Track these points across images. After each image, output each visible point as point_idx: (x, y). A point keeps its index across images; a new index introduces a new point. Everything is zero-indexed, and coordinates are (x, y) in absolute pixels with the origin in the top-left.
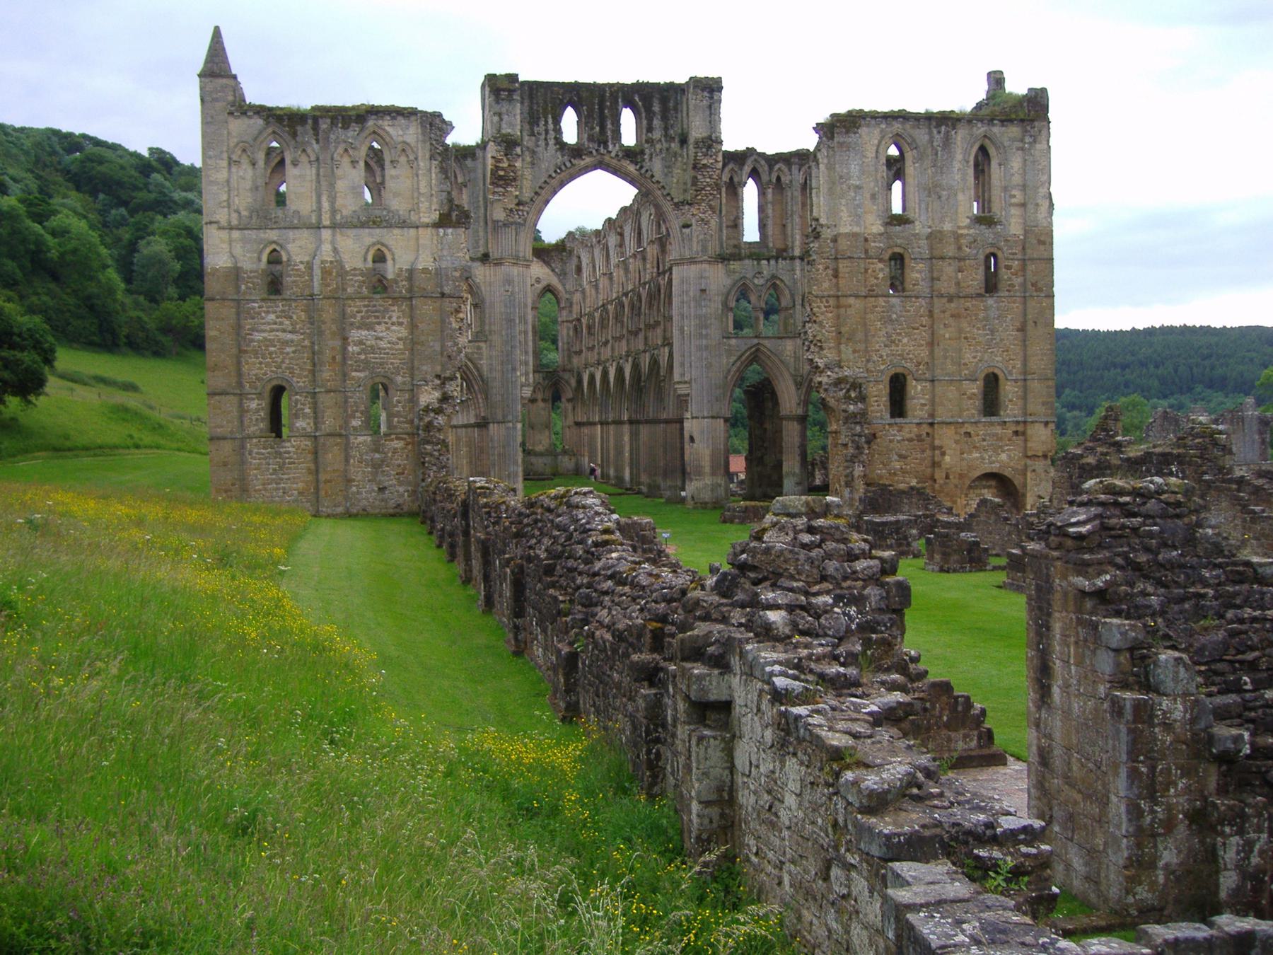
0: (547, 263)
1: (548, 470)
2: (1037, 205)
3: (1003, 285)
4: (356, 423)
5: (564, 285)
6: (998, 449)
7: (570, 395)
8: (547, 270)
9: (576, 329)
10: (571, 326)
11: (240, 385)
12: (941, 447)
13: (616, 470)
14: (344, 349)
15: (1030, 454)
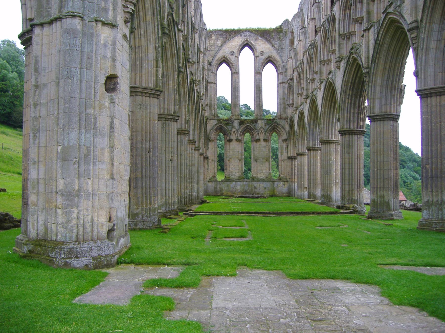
0: (269, 41)
1: (267, 193)
5: (281, 57)
7: (285, 137)
8: (268, 46)
9: (289, 87)
10: (286, 86)
13: (323, 189)
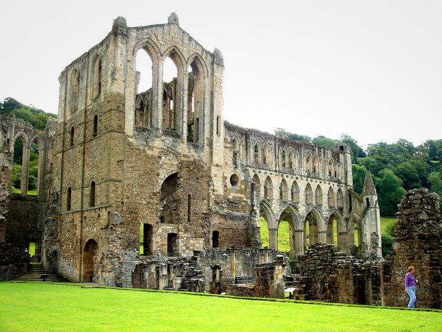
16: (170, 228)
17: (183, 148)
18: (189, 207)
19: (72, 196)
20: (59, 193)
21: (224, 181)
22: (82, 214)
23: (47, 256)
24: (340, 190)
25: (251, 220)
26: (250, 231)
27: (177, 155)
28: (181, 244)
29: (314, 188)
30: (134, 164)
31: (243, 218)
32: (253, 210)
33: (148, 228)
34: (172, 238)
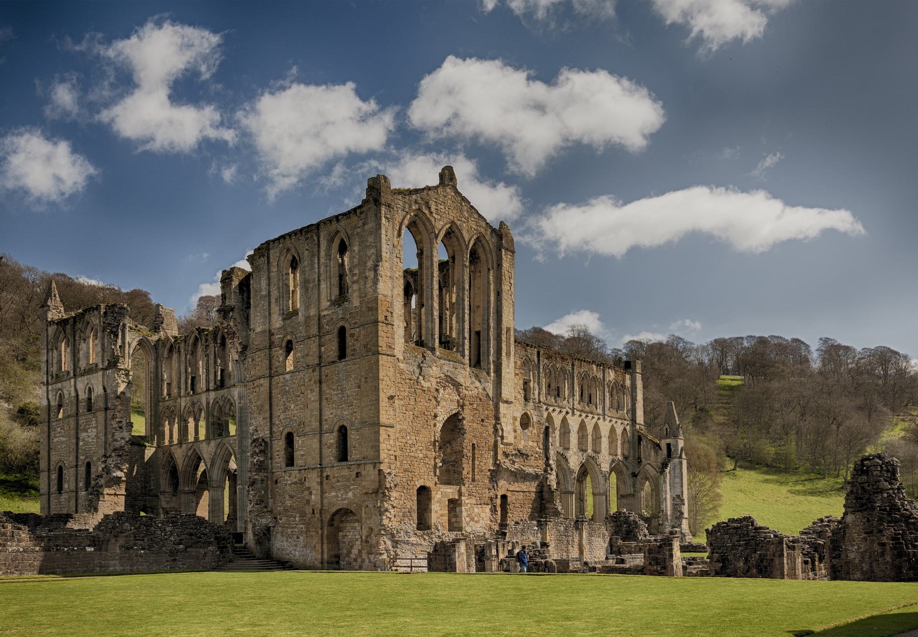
2: (366, 277)
3: (348, 351)
4: (81, 484)
6: (347, 488)
11: (49, 465)
12: (308, 489)
14: (77, 444)
15: (364, 491)
16: (450, 491)
17: (464, 375)
18: (473, 460)
19: (296, 446)
20: (268, 440)
21: (514, 424)
22: (322, 472)
23: (255, 535)
24: (625, 429)
25: (547, 478)
26: (546, 495)
27: (457, 385)
28: (464, 514)
29: (590, 429)
30: (407, 401)
31: (537, 476)
32: (549, 465)
33: (424, 492)
34: (454, 505)
